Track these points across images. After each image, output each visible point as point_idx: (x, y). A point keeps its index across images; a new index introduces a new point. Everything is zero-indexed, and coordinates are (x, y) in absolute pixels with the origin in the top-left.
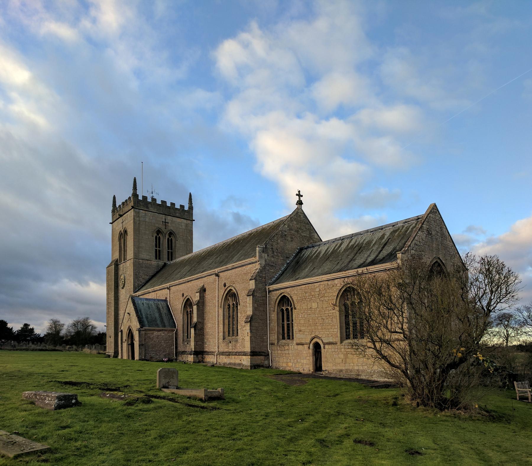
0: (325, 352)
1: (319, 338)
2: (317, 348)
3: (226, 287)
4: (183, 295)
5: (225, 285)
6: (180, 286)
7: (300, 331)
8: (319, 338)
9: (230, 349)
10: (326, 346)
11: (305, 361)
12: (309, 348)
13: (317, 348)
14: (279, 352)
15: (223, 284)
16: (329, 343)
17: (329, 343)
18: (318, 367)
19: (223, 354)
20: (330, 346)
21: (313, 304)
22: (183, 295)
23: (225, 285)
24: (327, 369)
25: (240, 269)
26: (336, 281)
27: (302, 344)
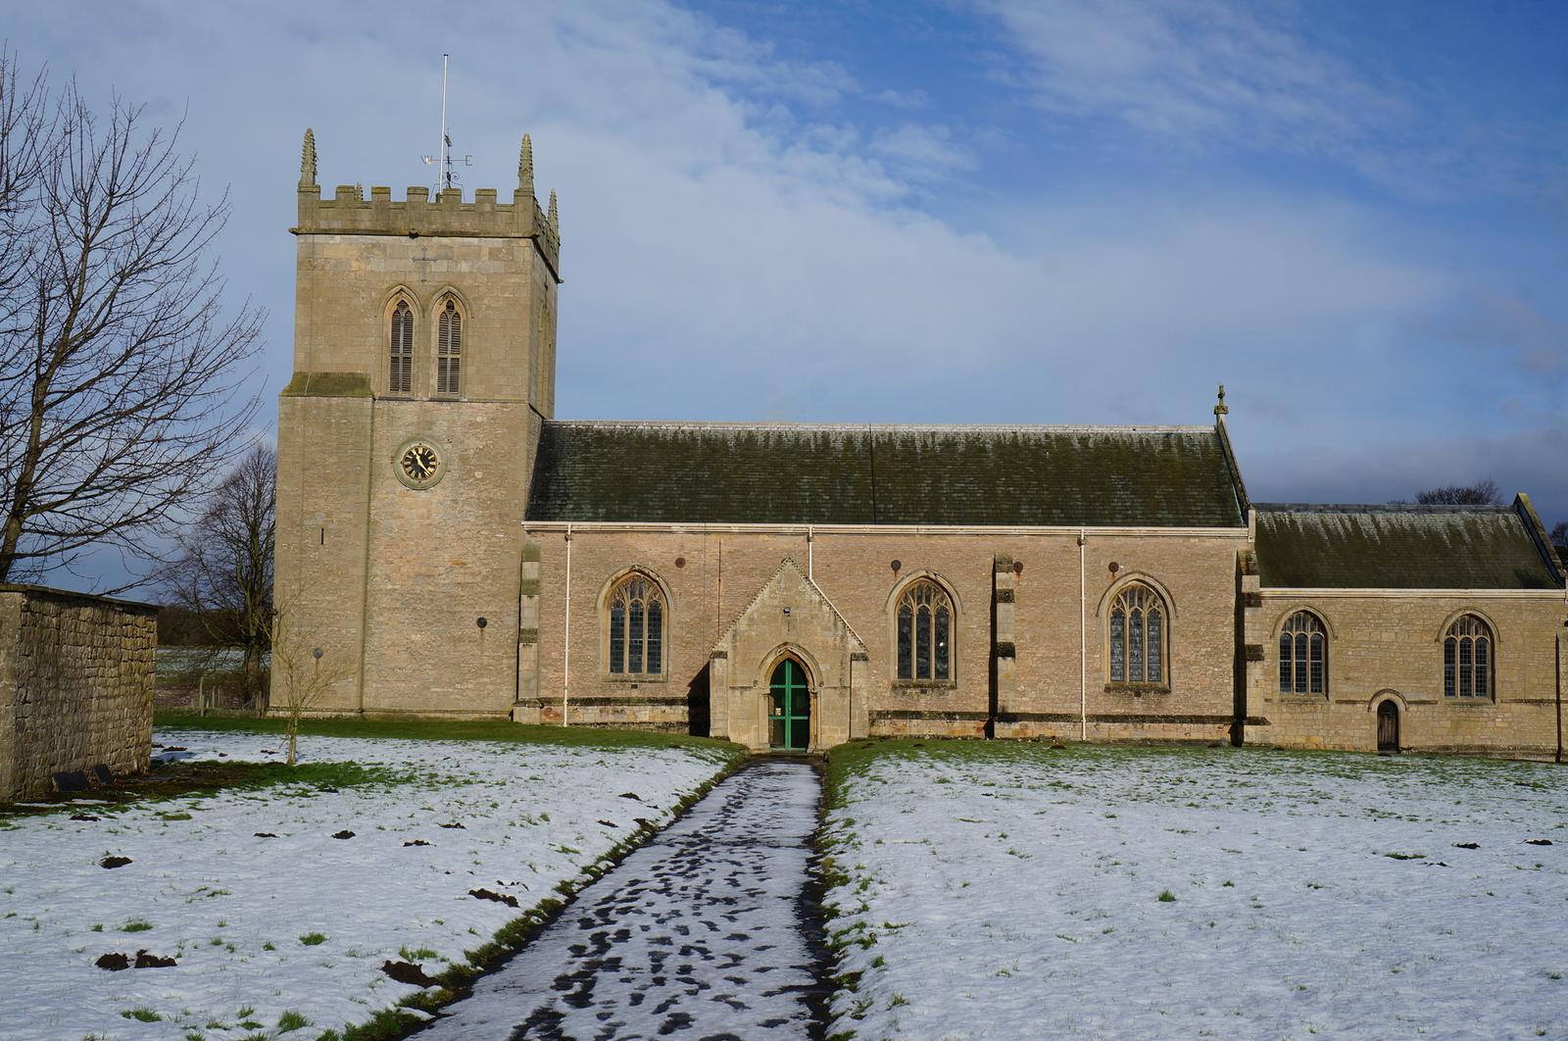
0: (1408, 715)
1: (1397, 694)
2: (1388, 711)
3: (1118, 574)
4: (896, 566)
5: (1113, 567)
6: (876, 540)
7: (1348, 679)
8: (1397, 694)
9: (1138, 707)
10: (1413, 708)
11: (1358, 734)
12: (1369, 708)
13: (1388, 711)
14: (1289, 716)
15: (1105, 563)
16: (1415, 703)
17: (1415, 703)
18: (1389, 745)
19: (1107, 718)
20: (1421, 708)
21: (1385, 635)
22: (896, 566)
23: (1113, 567)
24: (1411, 745)
25: (1176, 540)
26: (1442, 602)
27: (1354, 702)
